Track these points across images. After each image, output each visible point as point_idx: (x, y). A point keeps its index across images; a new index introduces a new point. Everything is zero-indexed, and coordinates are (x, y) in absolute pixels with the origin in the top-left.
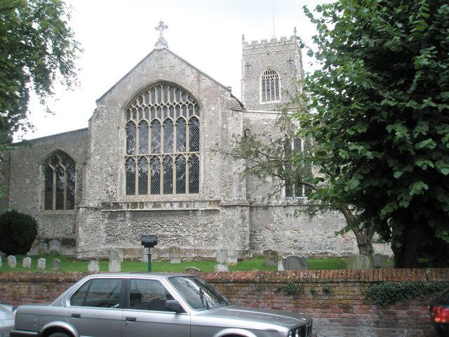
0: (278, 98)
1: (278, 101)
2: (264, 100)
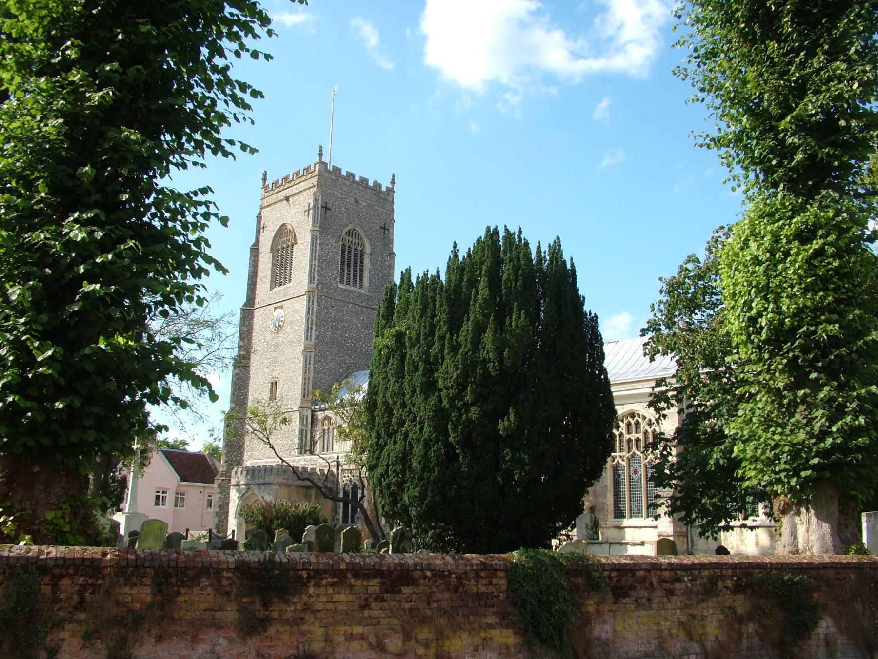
0: (361, 287)
1: (362, 291)
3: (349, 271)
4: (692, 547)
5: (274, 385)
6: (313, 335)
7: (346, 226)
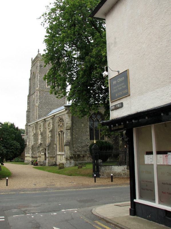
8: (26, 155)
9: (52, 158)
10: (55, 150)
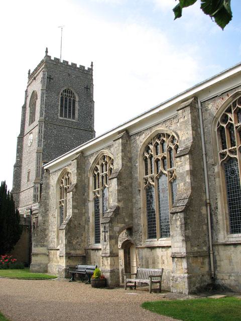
1: (74, 121)
2: (61, 116)
3: (66, 110)
4: (215, 268)
5: (29, 173)
6: (42, 144)
7: (63, 87)
8: (35, 250)
9: (200, 260)
10: (205, 227)
